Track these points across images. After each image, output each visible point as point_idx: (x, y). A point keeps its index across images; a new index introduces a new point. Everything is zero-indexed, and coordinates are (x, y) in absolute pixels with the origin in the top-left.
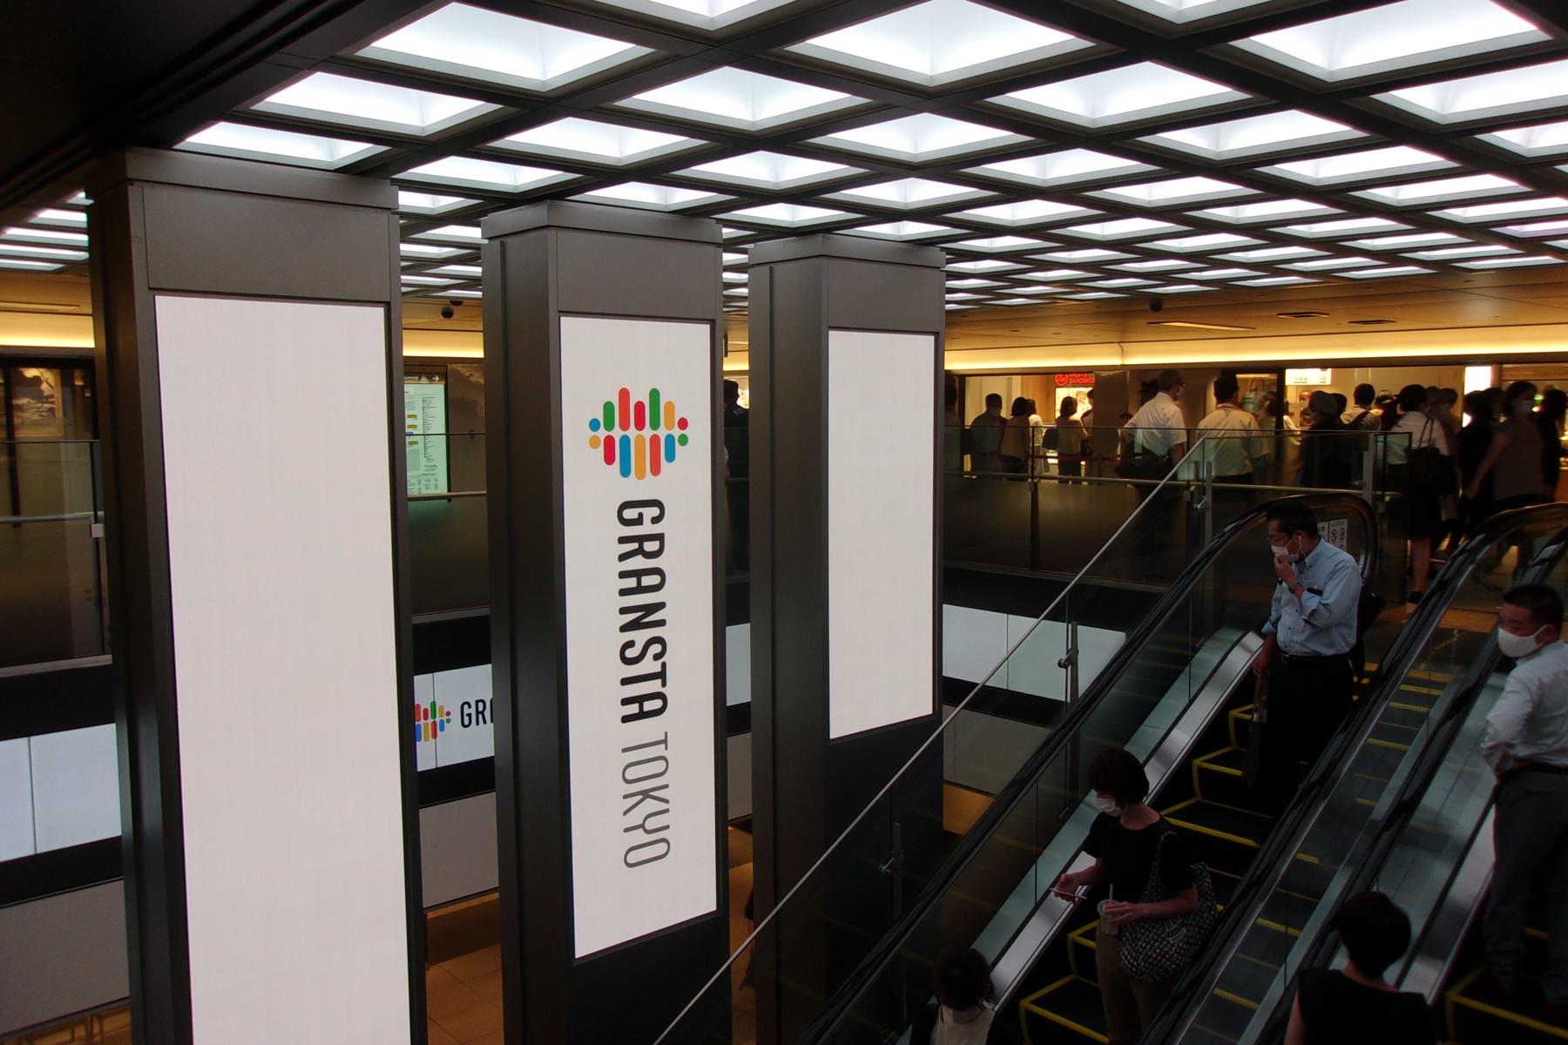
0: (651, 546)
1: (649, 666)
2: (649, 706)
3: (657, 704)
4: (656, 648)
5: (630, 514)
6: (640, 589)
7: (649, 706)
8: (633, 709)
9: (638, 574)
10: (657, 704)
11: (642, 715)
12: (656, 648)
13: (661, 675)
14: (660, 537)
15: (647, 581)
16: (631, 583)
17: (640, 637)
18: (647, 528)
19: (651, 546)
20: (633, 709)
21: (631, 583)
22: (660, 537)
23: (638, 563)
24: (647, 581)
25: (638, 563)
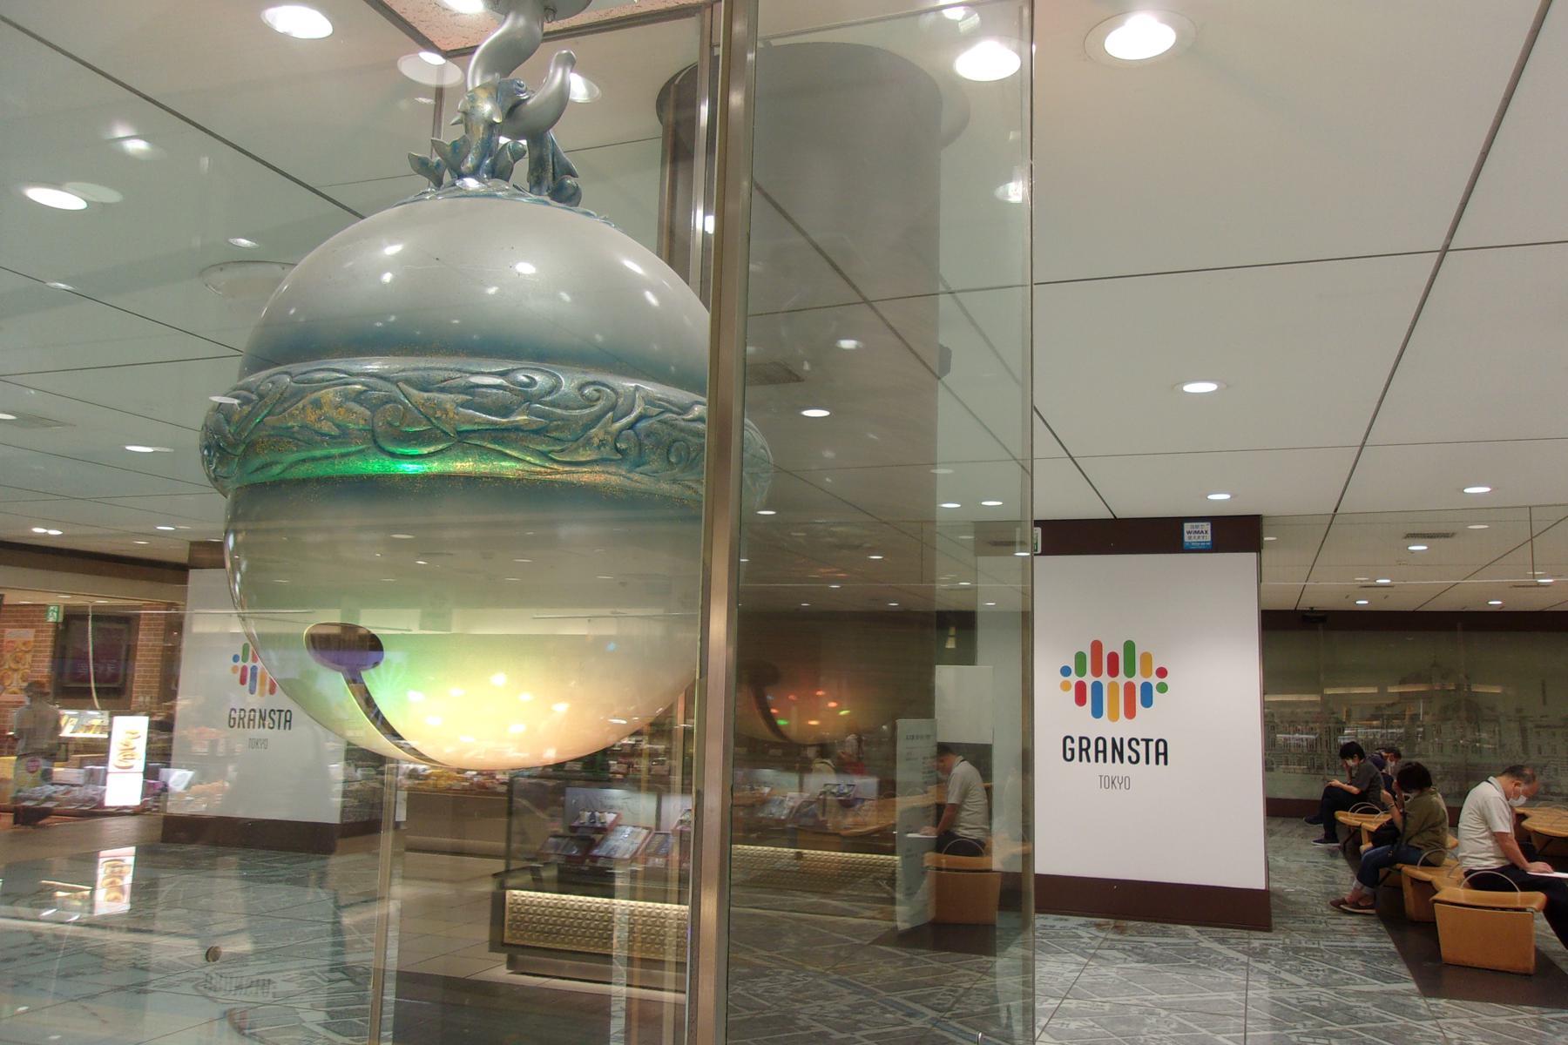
0: (1085, 745)
1: (1141, 749)
2: (1161, 750)
3: (1161, 745)
4: (1134, 743)
5: (1069, 755)
6: (1104, 751)
7: (1161, 750)
8: (1161, 758)
9: (1097, 752)
10: (1161, 745)
11: (1165, 754)
12: (1134, 743)
13: (1147, 741)
14: (1081, 739)
15: (1101, 748)
16: (1101, 756)
17: (1127, 752)
18: (1076, 746)
19: (1085, 745)
20: (1161, 758)
21: (1101, 756)
22: (1081, 739)
23: (1092, 751)
24: (1101, 748)
25: (1092, 751)
